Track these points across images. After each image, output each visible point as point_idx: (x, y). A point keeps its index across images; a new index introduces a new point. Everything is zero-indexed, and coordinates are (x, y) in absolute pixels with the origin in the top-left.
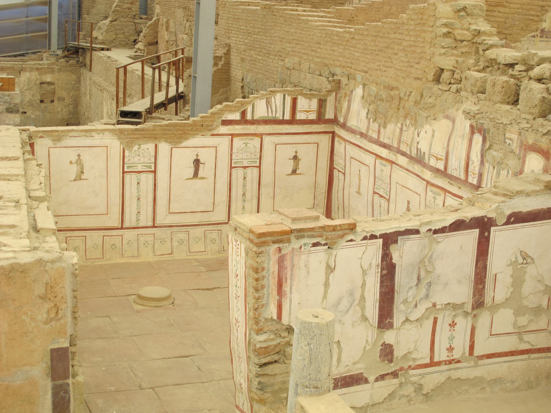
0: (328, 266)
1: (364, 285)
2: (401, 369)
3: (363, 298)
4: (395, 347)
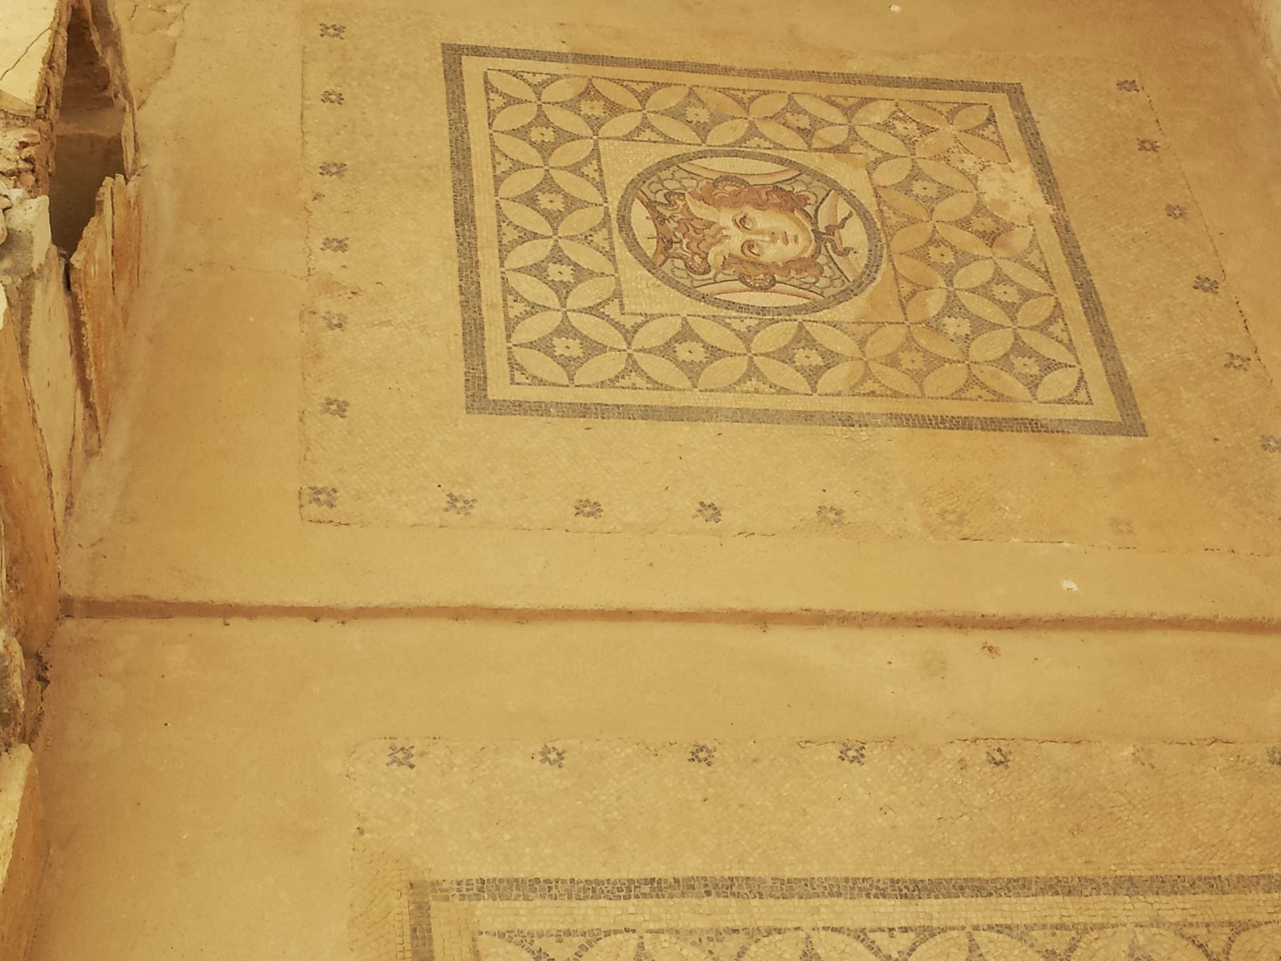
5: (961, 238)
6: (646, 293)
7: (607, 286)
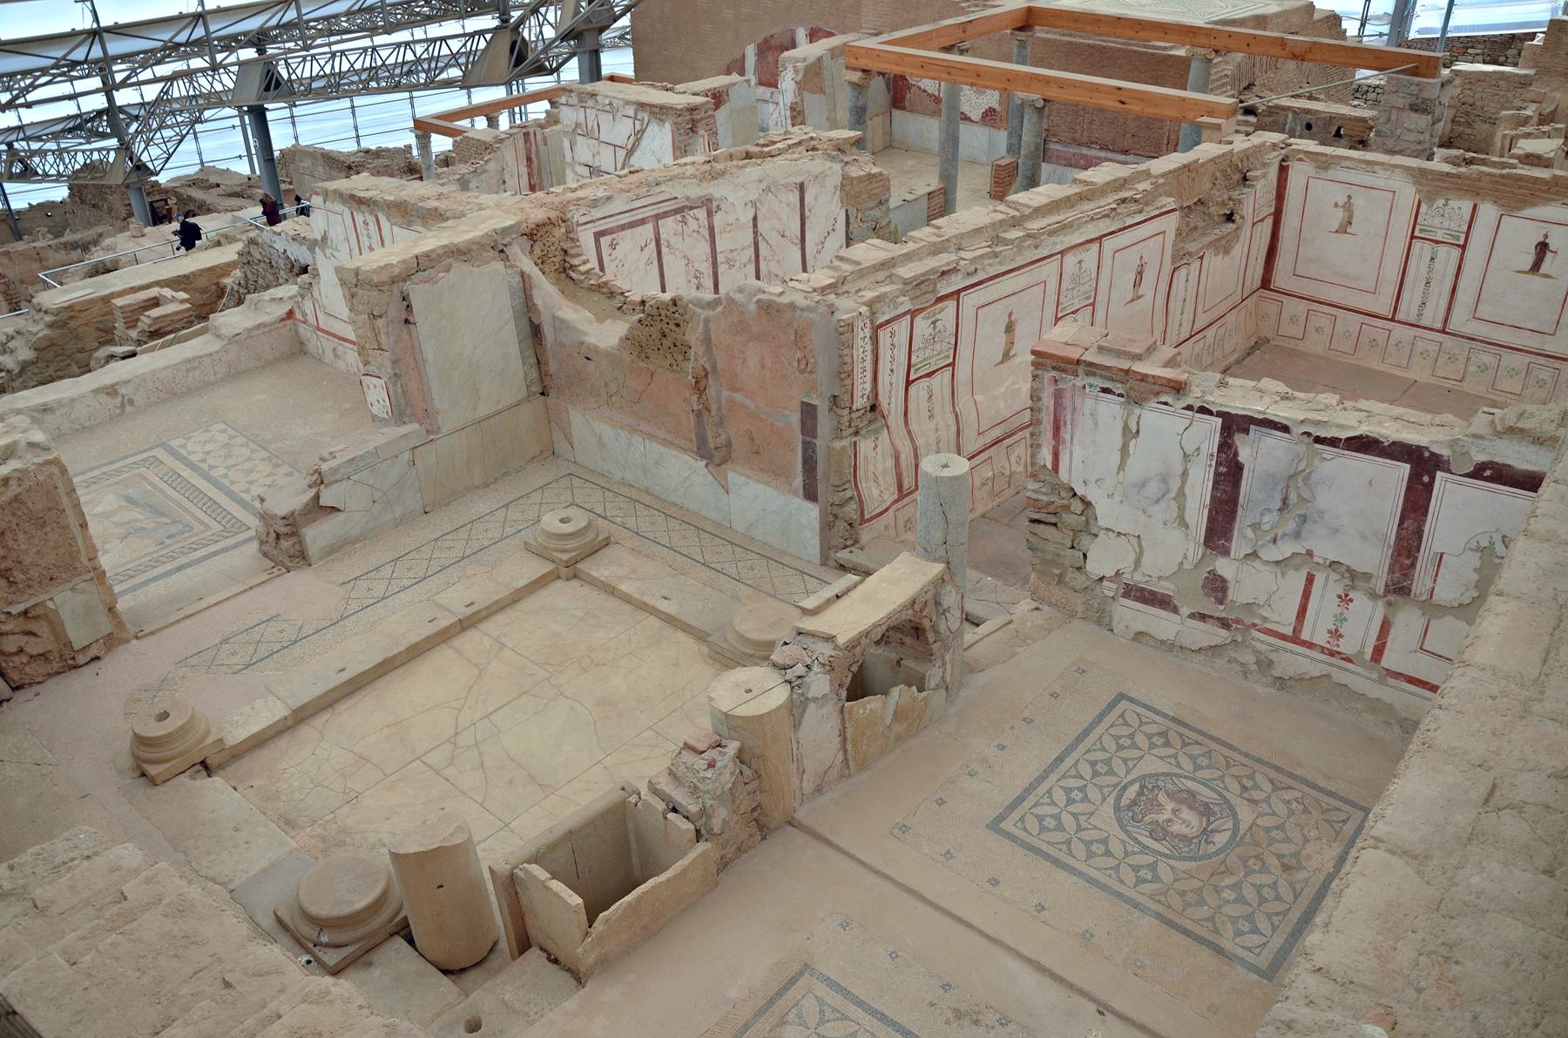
0: (1126, 428)
1: (1185, 474)
2: (1238, 621)
3: (1181, 494)
4: (1231, 585)
5: (1273, 862)
6: (1105, 819)
7: (1089, 808)
